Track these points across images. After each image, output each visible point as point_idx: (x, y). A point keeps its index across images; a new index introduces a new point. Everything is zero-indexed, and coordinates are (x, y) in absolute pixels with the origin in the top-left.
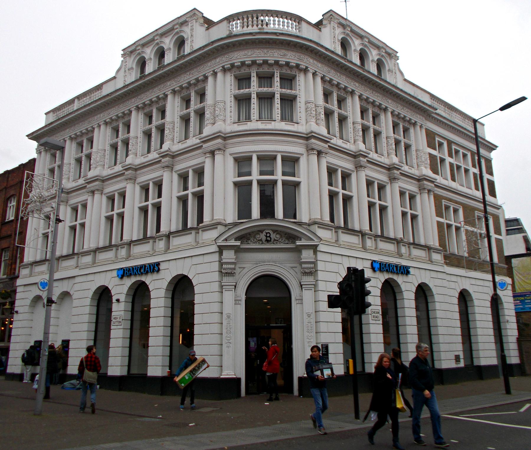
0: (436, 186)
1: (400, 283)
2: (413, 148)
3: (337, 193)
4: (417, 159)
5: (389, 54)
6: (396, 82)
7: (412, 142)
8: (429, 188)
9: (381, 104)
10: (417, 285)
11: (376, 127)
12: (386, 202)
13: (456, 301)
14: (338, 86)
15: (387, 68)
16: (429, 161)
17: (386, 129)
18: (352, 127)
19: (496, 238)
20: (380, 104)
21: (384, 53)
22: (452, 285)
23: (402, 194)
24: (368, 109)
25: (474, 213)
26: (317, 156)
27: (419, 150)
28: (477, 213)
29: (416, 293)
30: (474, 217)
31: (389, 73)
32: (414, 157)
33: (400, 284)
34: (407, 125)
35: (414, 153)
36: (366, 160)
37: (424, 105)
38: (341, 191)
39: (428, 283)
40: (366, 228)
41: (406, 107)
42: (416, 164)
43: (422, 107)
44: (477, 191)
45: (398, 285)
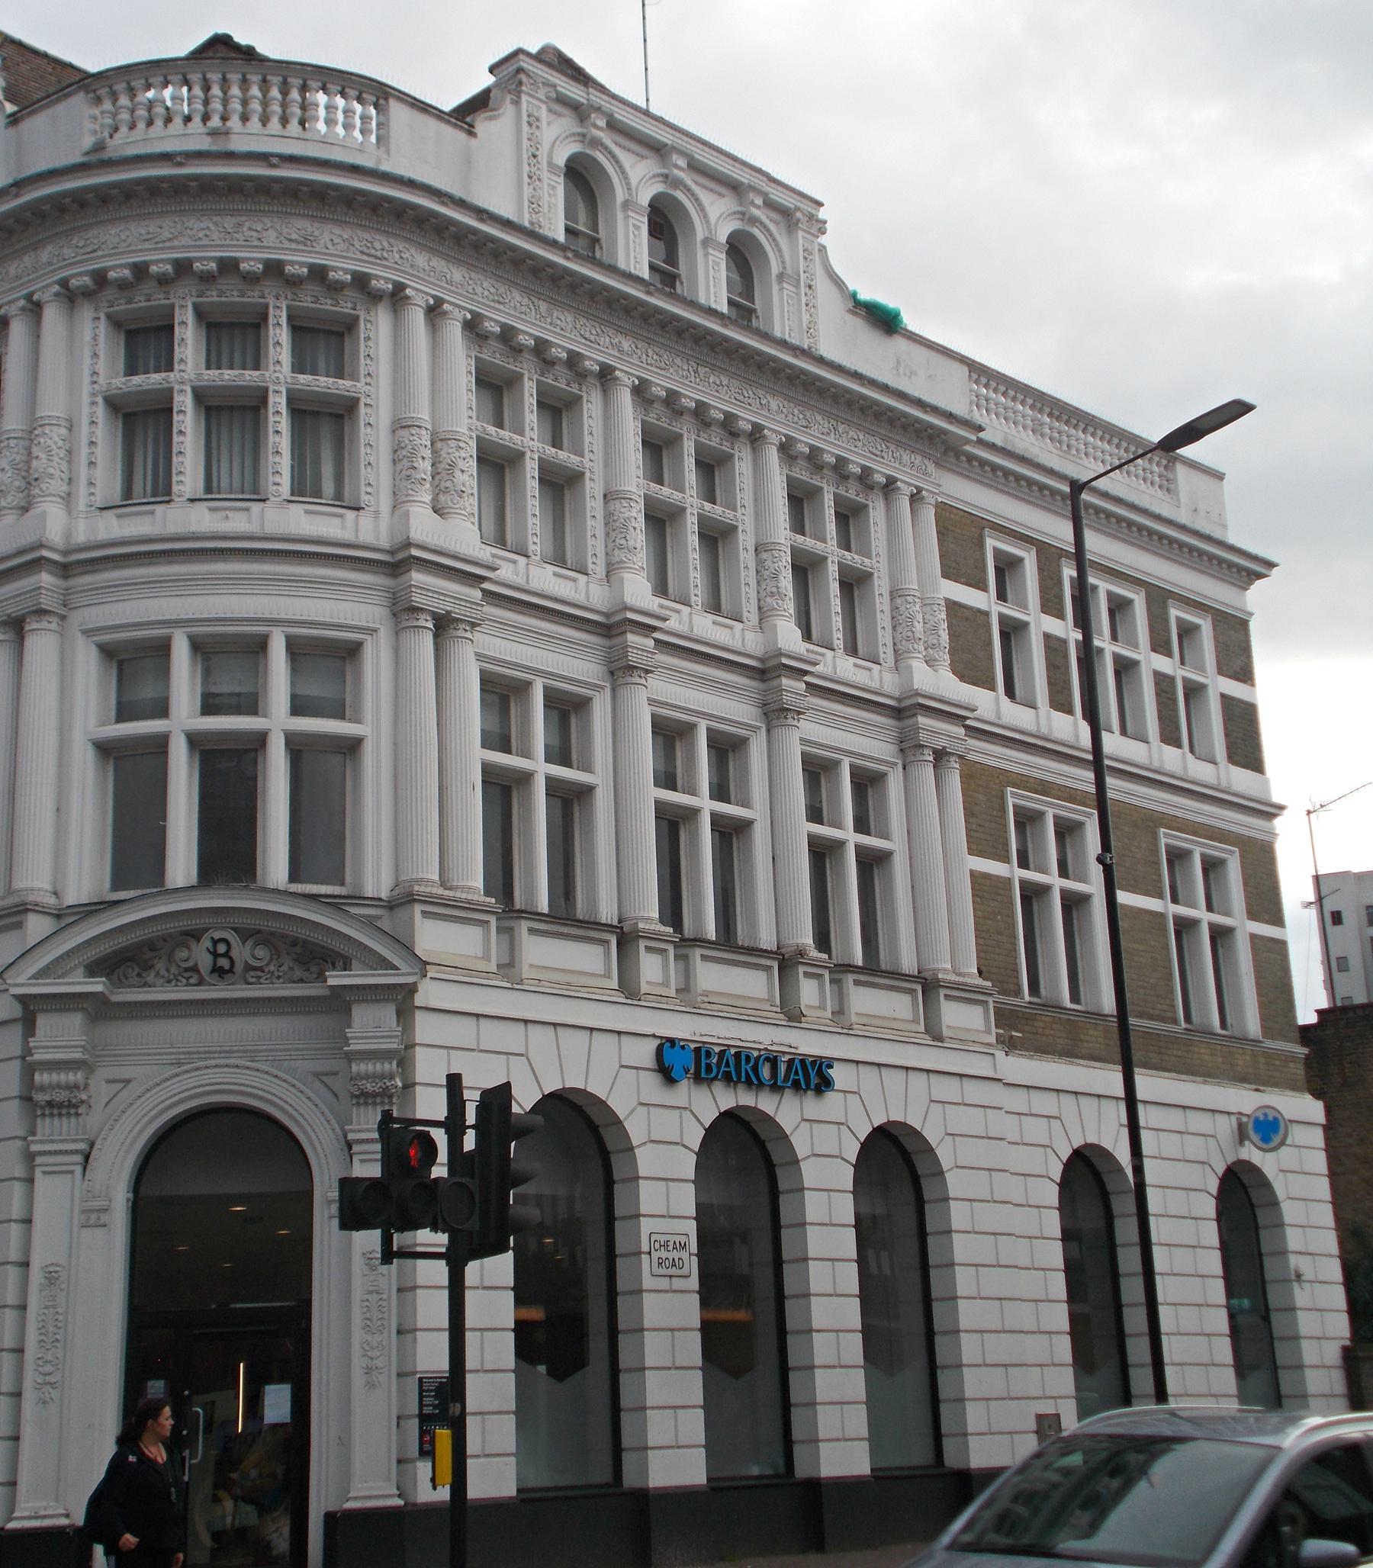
0: (974, 732)
1: (933, 1141)
2: (881, 585)
4: (894, 628)
5: (785, 213)
6: (811, 328)
7: (877, 563)
8: (941, 743)
10: (1065, 1153)
13: (1208, 1207)
15: (775, 269)
16: (945, 636)
17: (758, 515)
19: (1253, 937)
21: (758, 207)
22: (1036, 1131)
25: (1155, 838)
27: (901, 593)
28: (1166, 835)
29: (1066, 1185)
30: (1155, 851)
31: (781, 289)
32: (883, 620)
33: (1271, 1179)
35: (882, 604)
37: (926, 412)
39: (1110, 1148)
41: (849, 423)
42: (890, 650)
43: (918, 420)
44: (1170, 751)
45: (1266, 1184)
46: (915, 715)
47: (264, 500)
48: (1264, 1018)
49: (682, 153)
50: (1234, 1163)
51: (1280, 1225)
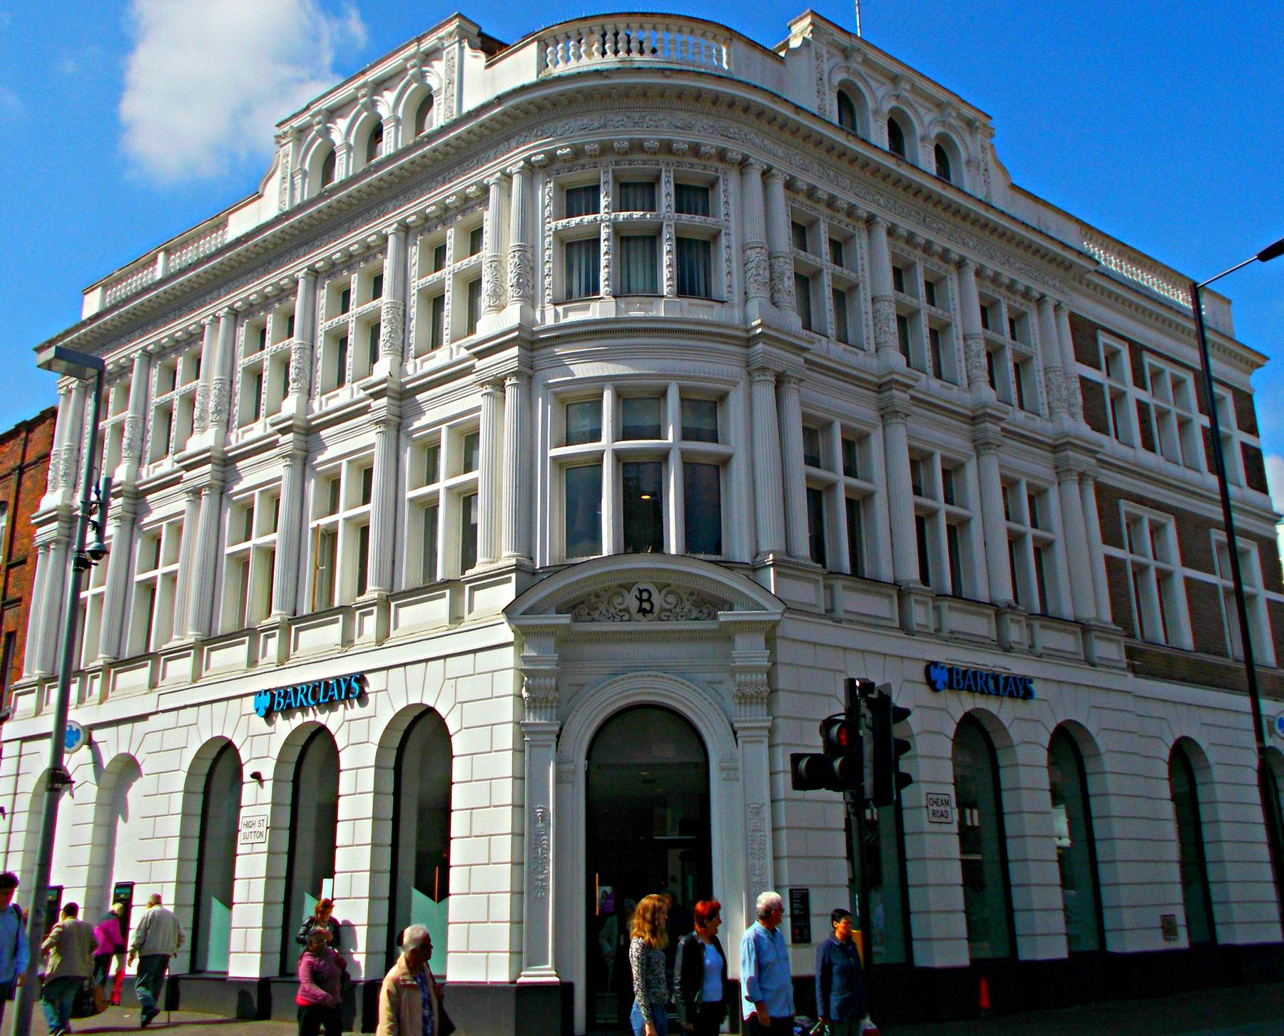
2: (1038, 364)
3: (933, 513)
9: (1000, 274)
12: (1049, 530)
14: (1011, 287)
17: (963, 315)
18: (1043, 379)
19: (1268, 601)
20: (1013, 282)
26: (1079, 484)
30: (1208, 542)
31: (969, 171)
35: (1040, 377)
36: (999, 429)
38: (1153, 564)
40: (1005, 593)
42: (1046, 406)
48: (1277, 655)
50: (1064, 722)
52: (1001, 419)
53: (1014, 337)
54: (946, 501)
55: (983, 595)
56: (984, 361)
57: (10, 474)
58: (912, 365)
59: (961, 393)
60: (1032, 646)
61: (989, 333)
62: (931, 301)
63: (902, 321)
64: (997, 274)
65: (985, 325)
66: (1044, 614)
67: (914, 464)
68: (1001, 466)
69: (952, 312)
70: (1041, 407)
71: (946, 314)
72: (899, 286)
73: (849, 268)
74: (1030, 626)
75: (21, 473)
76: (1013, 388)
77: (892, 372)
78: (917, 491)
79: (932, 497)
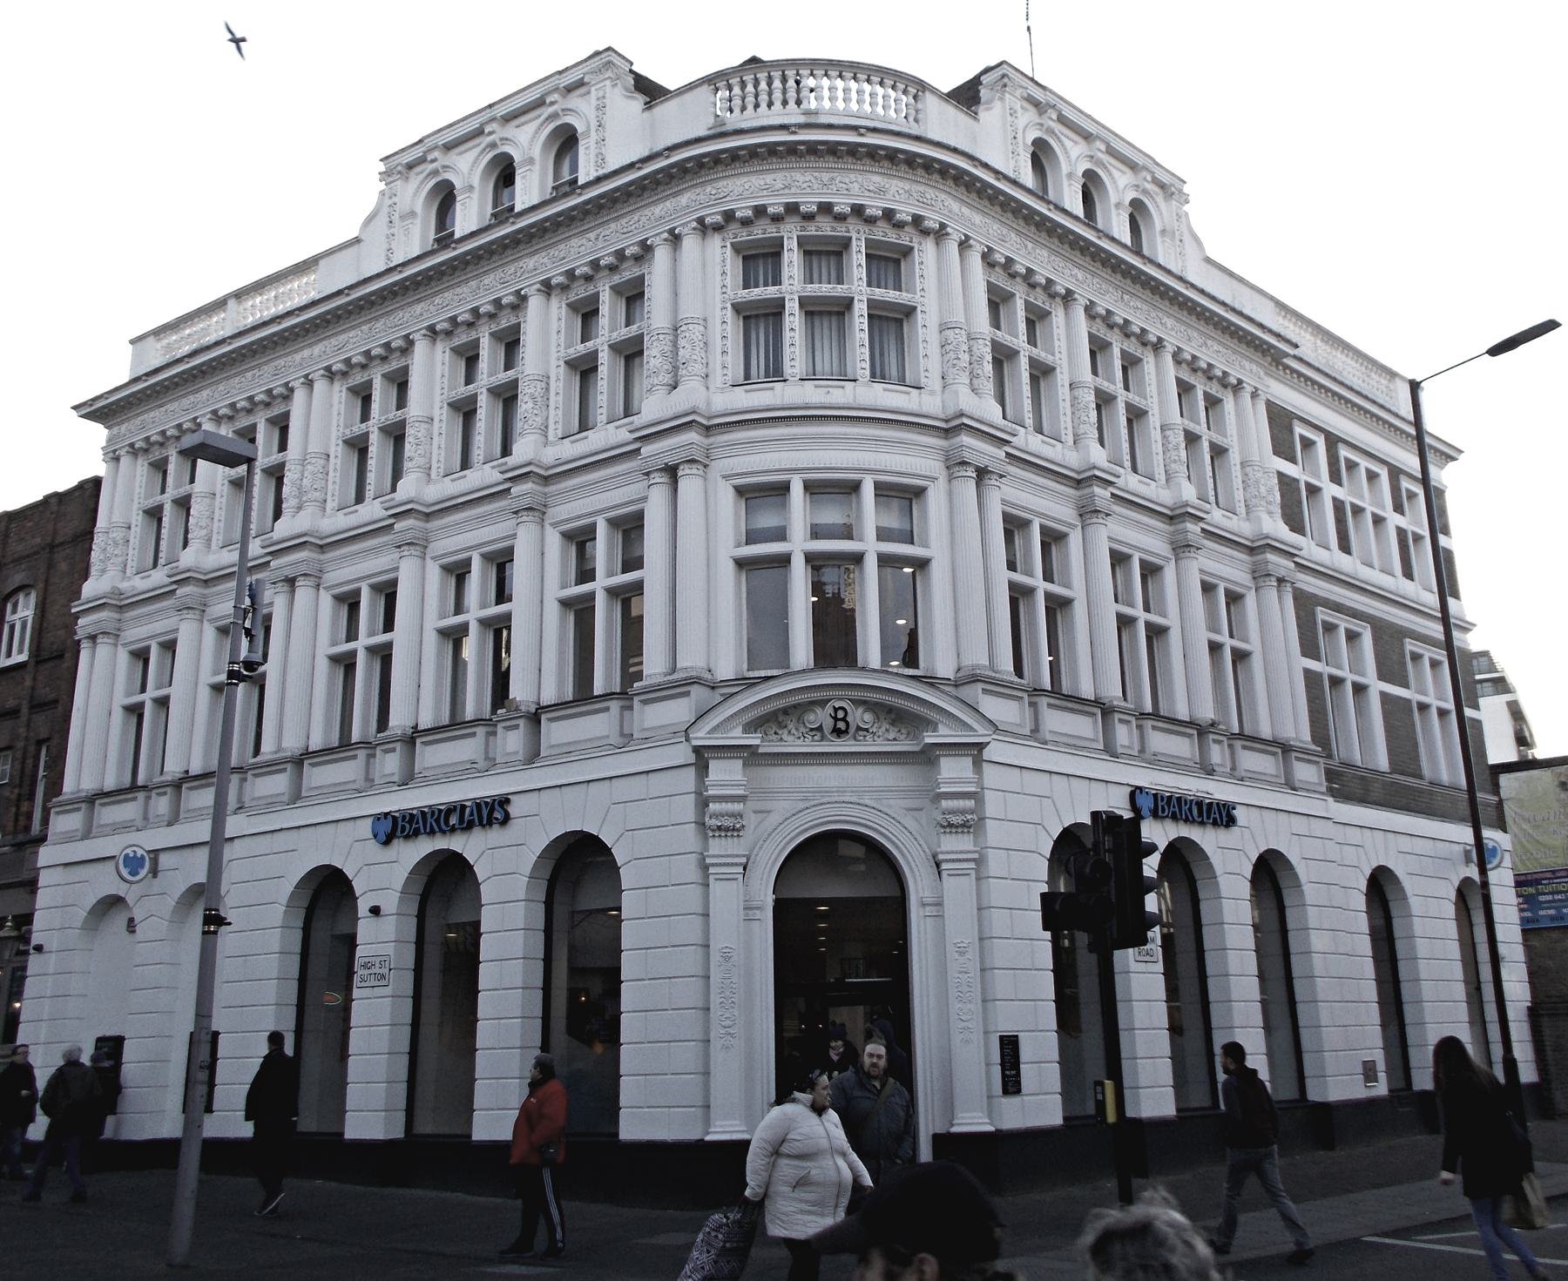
2: (1234, 457)
5: (1162, 186)
7: (1231, 441)
8: (1282, 573)
11: (1040, 353)
13: (1360, 902)
15: (1158, 226)
17: (1161, 402)
21: (1148, 182)
22: (1350, 855)
23: (1119, 560)
24: (1013, 295)
31: (1163, 242)
34: (1039, 299)
46: (1264, 552)
47: (785, 381)
49: (1103, 141)
51: (1409, 916)
52: (1111, 483)
53: (1127, 388)
54: (1045, 580)
55: (1087, 691)
56: (1094, 414)
57: (36, 553)
58: (1009, 417)
59: (1066, 450)
60: (1036, 730)
61: (1131, 395)
62: (1032, 341)
63: (998, 363)
64: (1050, 282)
65: (1095, 372)
66: (1055, 691)
67: (1009, 536)
68: (1004, 502)
69: (1058, 355)
70: (1063, 433)
71: (1050, 358)
72: (996, 323)
73: (907, 291)
74: (1033, 705)
75: (51, 552)
76: (1126, 446)
77: (962, 415)
78: (1012, 566)
79: (1030, 574)
